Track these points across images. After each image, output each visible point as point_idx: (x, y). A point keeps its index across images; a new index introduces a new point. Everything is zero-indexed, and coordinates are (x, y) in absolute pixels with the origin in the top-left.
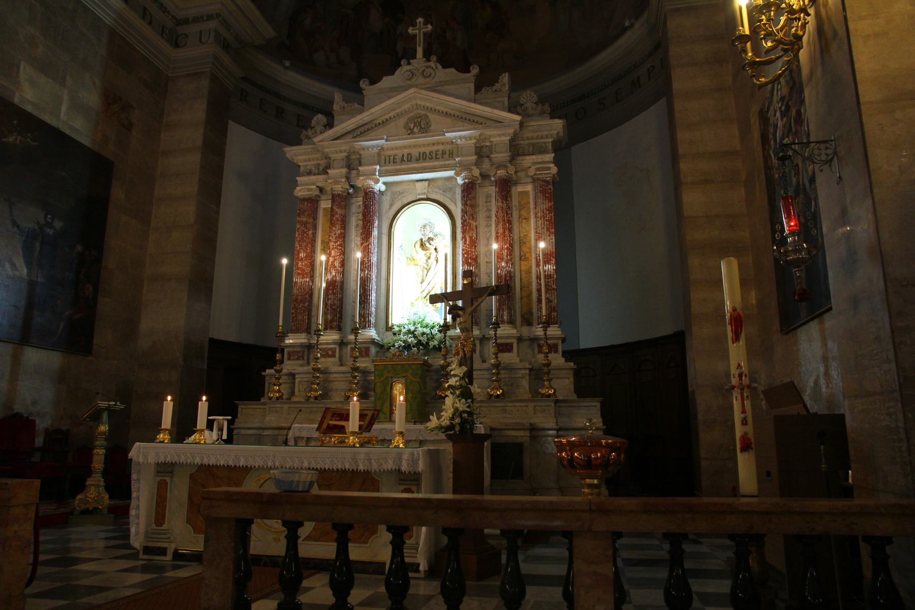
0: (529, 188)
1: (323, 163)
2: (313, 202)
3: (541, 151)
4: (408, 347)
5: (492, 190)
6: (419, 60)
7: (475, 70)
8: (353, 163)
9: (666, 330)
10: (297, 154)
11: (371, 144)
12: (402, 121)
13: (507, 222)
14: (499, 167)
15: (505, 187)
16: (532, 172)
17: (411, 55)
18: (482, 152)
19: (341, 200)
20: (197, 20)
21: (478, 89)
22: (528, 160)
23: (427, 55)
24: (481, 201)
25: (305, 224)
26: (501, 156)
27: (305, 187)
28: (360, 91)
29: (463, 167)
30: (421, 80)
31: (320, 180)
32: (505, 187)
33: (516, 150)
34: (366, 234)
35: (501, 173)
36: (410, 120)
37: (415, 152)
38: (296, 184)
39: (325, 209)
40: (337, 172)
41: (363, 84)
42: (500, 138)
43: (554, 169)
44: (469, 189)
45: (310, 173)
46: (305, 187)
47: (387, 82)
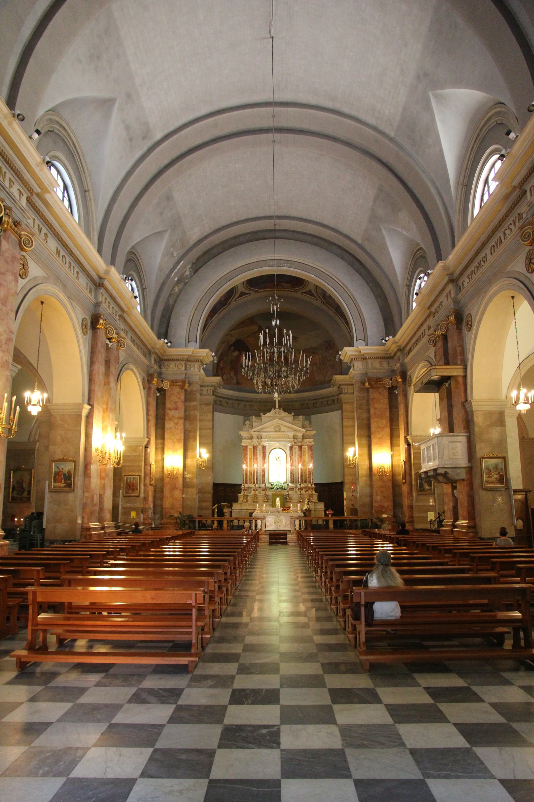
0: (306, 447)
1: (250, 436)
2: (247, 447)
3: (310, 438)
4: (277, 489)
5: (297, 447)
6: (277, 410)
7: (293, 414)
8: (260, 438)
9: (339, 481)
10: (243, 434)
11: (264, 434)
12: (273, 427)
13: (301, 456)
14: (300, 442)
15: (300, 447)
16: (307, 443)
17: (275, 408)
18: (295, 437)
19: (255, 448)
20: (207, 386)
21: (294, 420)
22: (306, 440)
23: (279, 408)
24: (294, 449)
25: (245, 453)
26: (300, 440)
27: (244, 443)
28: (261, 416)
29: (290, 442)
30: (277, 415)
31: (249, 441)
32: (300, 447)
33: (304, 437)
34: (264, 457)
35: (300, 444)
36: (275, 427)
37: (277, 436)
38: (242, 442)
39: (250, 449)
40: (255, 440)
41: (261, 414)
42: (300, 435)
43: (313, 443)
44: (291, 448)
45: (246, 439)
46: (244, 443)
47: (268, 414)
